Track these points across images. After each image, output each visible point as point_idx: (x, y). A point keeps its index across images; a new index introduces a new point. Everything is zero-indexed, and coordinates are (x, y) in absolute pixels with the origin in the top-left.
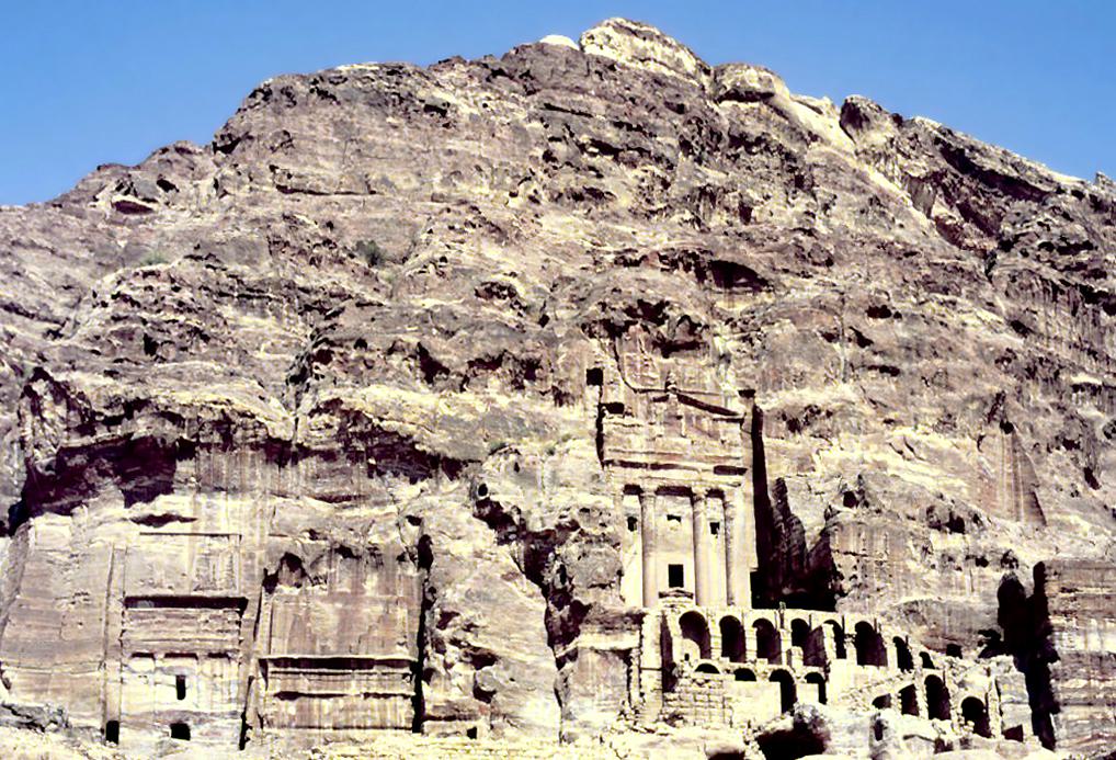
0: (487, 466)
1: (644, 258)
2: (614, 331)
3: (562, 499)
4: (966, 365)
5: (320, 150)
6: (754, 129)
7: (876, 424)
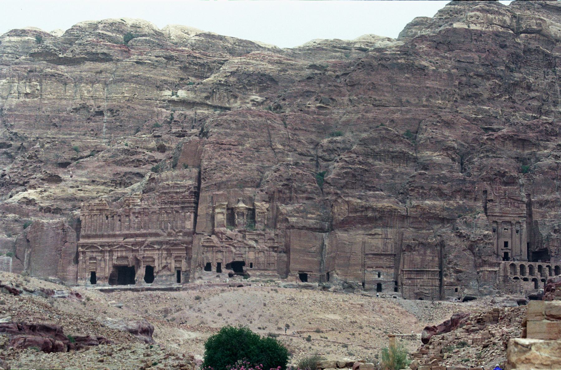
0: (458, 221)
1: (496, 138)
3: (478, 232)
5: (385, 89)
6: (534, 45)
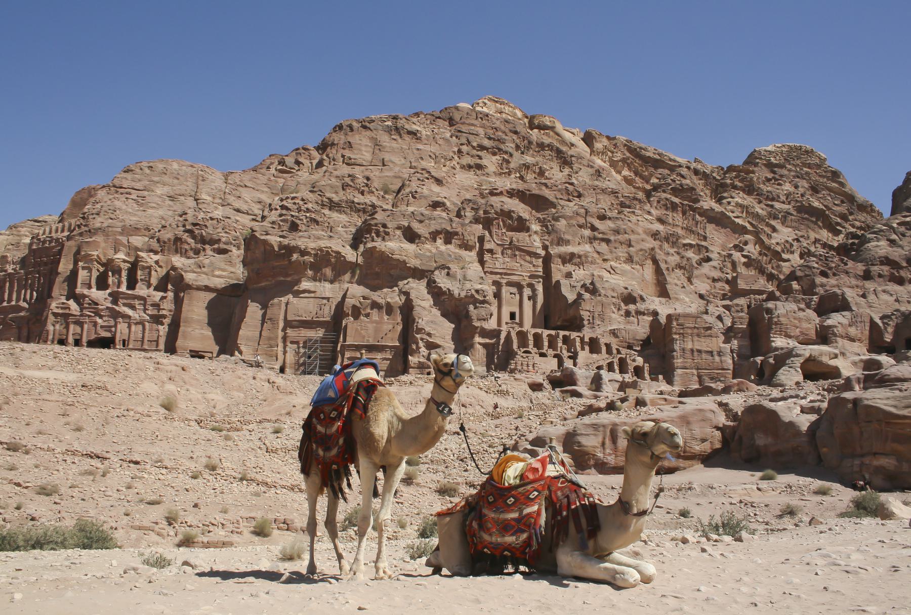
4: (638, 237)
5: (363, 148)
6: (547, 140)
7: (599, 261)
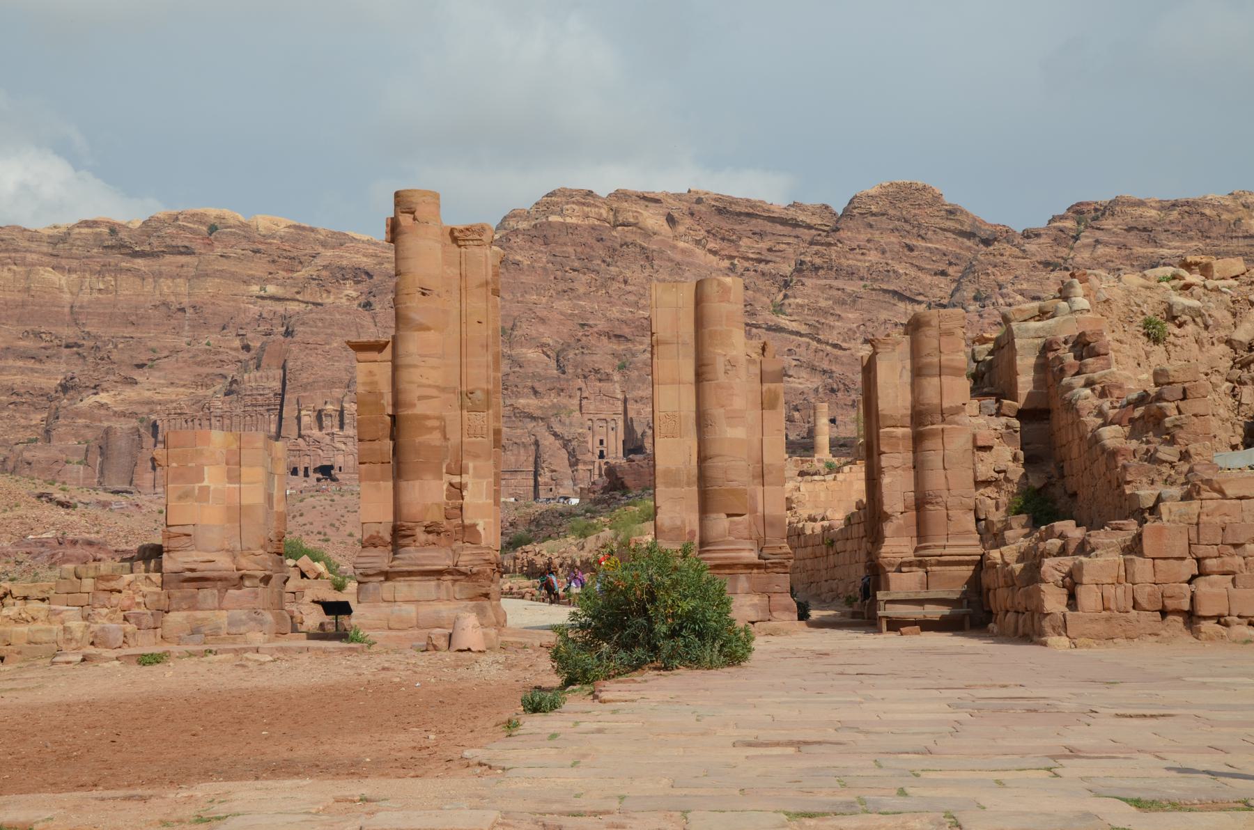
2: (585, 377)
